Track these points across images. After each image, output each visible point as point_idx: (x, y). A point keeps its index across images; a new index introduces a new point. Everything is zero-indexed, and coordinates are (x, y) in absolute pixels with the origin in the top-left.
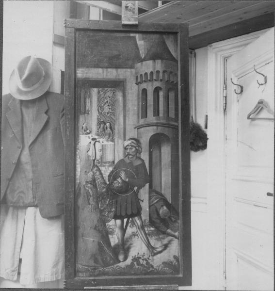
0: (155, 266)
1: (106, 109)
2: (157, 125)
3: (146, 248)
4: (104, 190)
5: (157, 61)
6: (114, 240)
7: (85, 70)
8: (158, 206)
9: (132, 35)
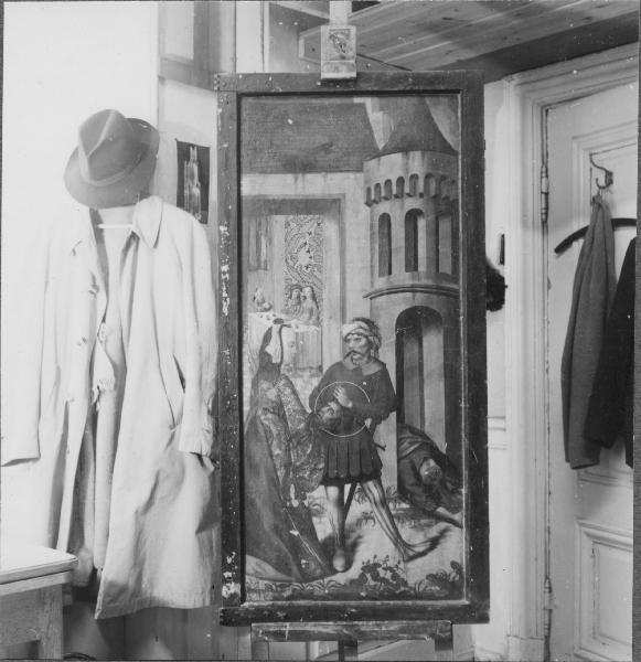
0: (411, 583)
1: (303, 258)
2: (413, 289)
3: (392, 546)
4: (302, 425)
5: (411, 154)
6: (324, 527)
7: (258, 178)
8: (417, 459)
9: (357, 100)
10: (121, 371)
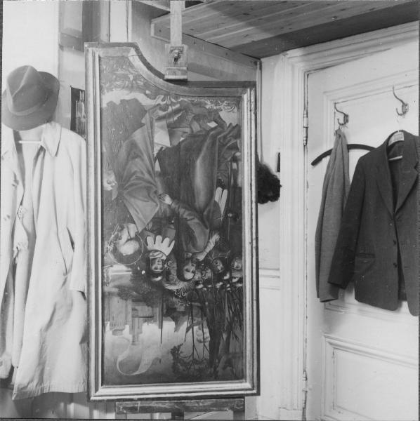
10: (32, 238)
